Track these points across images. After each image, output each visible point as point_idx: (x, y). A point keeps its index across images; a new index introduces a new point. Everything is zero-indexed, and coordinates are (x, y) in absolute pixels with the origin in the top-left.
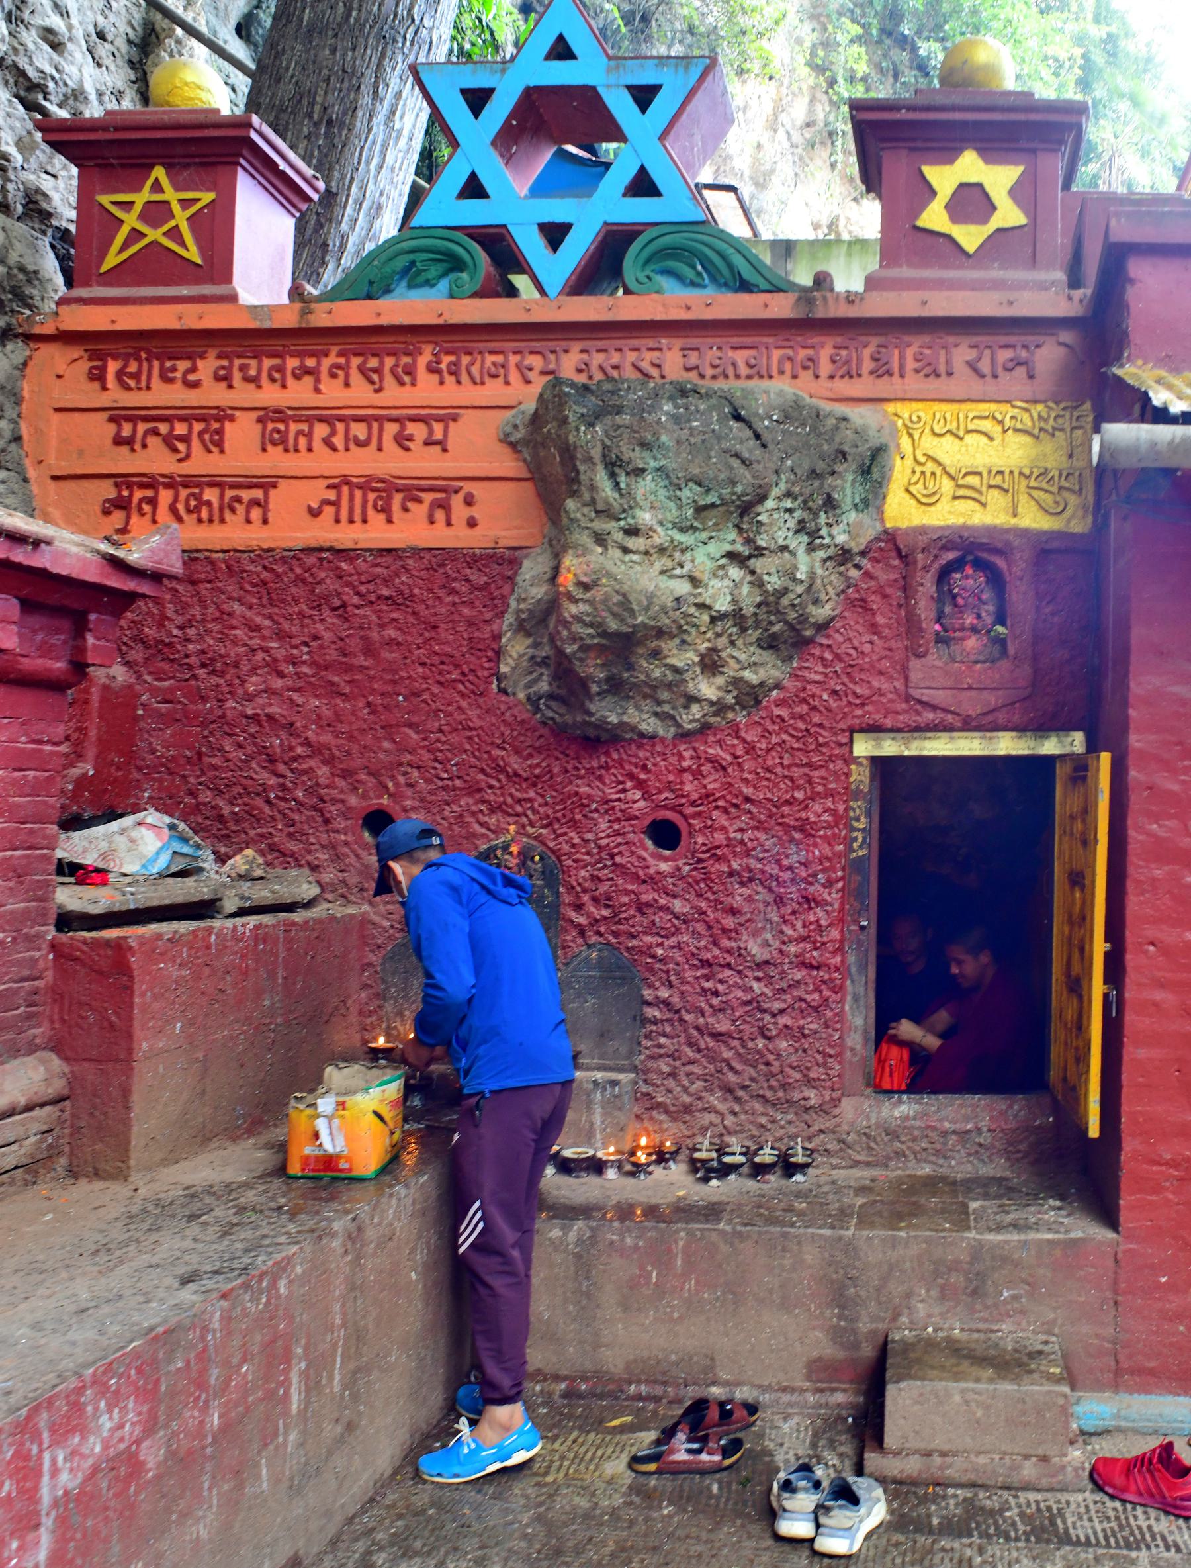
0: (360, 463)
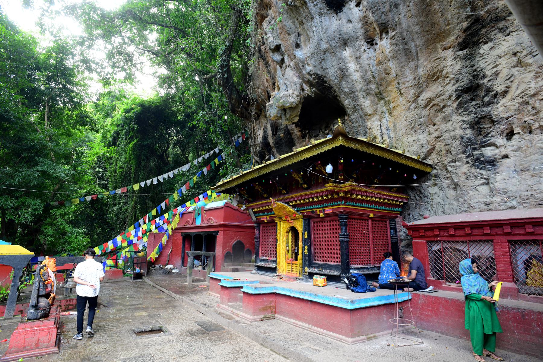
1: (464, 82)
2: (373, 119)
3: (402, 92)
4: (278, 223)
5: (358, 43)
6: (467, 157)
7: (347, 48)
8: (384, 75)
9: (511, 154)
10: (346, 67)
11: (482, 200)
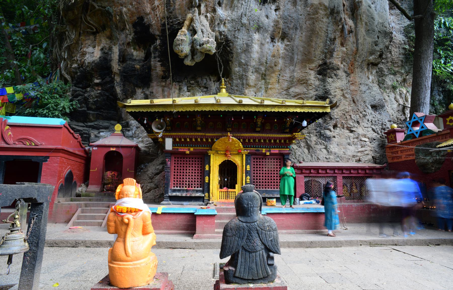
0: (407, 153)
1: (321, 93)
2: (251, 89)
3: (280, 81)
4: (212, 156)
5: (266, 34)
6: (317, 133)
7: (257, 33)
8: (273, 65)
9: (336, 136)
10: (252, 45)
11: (324, 156)
